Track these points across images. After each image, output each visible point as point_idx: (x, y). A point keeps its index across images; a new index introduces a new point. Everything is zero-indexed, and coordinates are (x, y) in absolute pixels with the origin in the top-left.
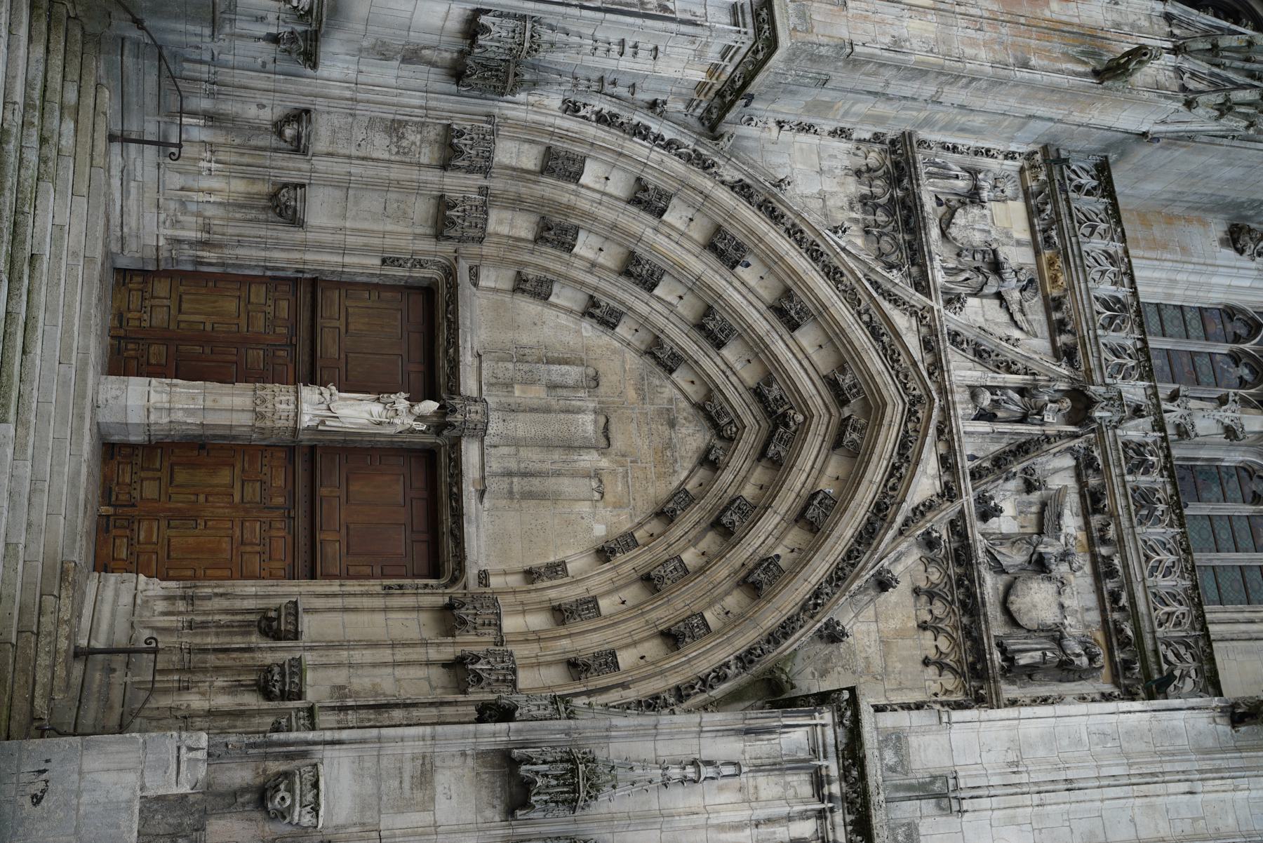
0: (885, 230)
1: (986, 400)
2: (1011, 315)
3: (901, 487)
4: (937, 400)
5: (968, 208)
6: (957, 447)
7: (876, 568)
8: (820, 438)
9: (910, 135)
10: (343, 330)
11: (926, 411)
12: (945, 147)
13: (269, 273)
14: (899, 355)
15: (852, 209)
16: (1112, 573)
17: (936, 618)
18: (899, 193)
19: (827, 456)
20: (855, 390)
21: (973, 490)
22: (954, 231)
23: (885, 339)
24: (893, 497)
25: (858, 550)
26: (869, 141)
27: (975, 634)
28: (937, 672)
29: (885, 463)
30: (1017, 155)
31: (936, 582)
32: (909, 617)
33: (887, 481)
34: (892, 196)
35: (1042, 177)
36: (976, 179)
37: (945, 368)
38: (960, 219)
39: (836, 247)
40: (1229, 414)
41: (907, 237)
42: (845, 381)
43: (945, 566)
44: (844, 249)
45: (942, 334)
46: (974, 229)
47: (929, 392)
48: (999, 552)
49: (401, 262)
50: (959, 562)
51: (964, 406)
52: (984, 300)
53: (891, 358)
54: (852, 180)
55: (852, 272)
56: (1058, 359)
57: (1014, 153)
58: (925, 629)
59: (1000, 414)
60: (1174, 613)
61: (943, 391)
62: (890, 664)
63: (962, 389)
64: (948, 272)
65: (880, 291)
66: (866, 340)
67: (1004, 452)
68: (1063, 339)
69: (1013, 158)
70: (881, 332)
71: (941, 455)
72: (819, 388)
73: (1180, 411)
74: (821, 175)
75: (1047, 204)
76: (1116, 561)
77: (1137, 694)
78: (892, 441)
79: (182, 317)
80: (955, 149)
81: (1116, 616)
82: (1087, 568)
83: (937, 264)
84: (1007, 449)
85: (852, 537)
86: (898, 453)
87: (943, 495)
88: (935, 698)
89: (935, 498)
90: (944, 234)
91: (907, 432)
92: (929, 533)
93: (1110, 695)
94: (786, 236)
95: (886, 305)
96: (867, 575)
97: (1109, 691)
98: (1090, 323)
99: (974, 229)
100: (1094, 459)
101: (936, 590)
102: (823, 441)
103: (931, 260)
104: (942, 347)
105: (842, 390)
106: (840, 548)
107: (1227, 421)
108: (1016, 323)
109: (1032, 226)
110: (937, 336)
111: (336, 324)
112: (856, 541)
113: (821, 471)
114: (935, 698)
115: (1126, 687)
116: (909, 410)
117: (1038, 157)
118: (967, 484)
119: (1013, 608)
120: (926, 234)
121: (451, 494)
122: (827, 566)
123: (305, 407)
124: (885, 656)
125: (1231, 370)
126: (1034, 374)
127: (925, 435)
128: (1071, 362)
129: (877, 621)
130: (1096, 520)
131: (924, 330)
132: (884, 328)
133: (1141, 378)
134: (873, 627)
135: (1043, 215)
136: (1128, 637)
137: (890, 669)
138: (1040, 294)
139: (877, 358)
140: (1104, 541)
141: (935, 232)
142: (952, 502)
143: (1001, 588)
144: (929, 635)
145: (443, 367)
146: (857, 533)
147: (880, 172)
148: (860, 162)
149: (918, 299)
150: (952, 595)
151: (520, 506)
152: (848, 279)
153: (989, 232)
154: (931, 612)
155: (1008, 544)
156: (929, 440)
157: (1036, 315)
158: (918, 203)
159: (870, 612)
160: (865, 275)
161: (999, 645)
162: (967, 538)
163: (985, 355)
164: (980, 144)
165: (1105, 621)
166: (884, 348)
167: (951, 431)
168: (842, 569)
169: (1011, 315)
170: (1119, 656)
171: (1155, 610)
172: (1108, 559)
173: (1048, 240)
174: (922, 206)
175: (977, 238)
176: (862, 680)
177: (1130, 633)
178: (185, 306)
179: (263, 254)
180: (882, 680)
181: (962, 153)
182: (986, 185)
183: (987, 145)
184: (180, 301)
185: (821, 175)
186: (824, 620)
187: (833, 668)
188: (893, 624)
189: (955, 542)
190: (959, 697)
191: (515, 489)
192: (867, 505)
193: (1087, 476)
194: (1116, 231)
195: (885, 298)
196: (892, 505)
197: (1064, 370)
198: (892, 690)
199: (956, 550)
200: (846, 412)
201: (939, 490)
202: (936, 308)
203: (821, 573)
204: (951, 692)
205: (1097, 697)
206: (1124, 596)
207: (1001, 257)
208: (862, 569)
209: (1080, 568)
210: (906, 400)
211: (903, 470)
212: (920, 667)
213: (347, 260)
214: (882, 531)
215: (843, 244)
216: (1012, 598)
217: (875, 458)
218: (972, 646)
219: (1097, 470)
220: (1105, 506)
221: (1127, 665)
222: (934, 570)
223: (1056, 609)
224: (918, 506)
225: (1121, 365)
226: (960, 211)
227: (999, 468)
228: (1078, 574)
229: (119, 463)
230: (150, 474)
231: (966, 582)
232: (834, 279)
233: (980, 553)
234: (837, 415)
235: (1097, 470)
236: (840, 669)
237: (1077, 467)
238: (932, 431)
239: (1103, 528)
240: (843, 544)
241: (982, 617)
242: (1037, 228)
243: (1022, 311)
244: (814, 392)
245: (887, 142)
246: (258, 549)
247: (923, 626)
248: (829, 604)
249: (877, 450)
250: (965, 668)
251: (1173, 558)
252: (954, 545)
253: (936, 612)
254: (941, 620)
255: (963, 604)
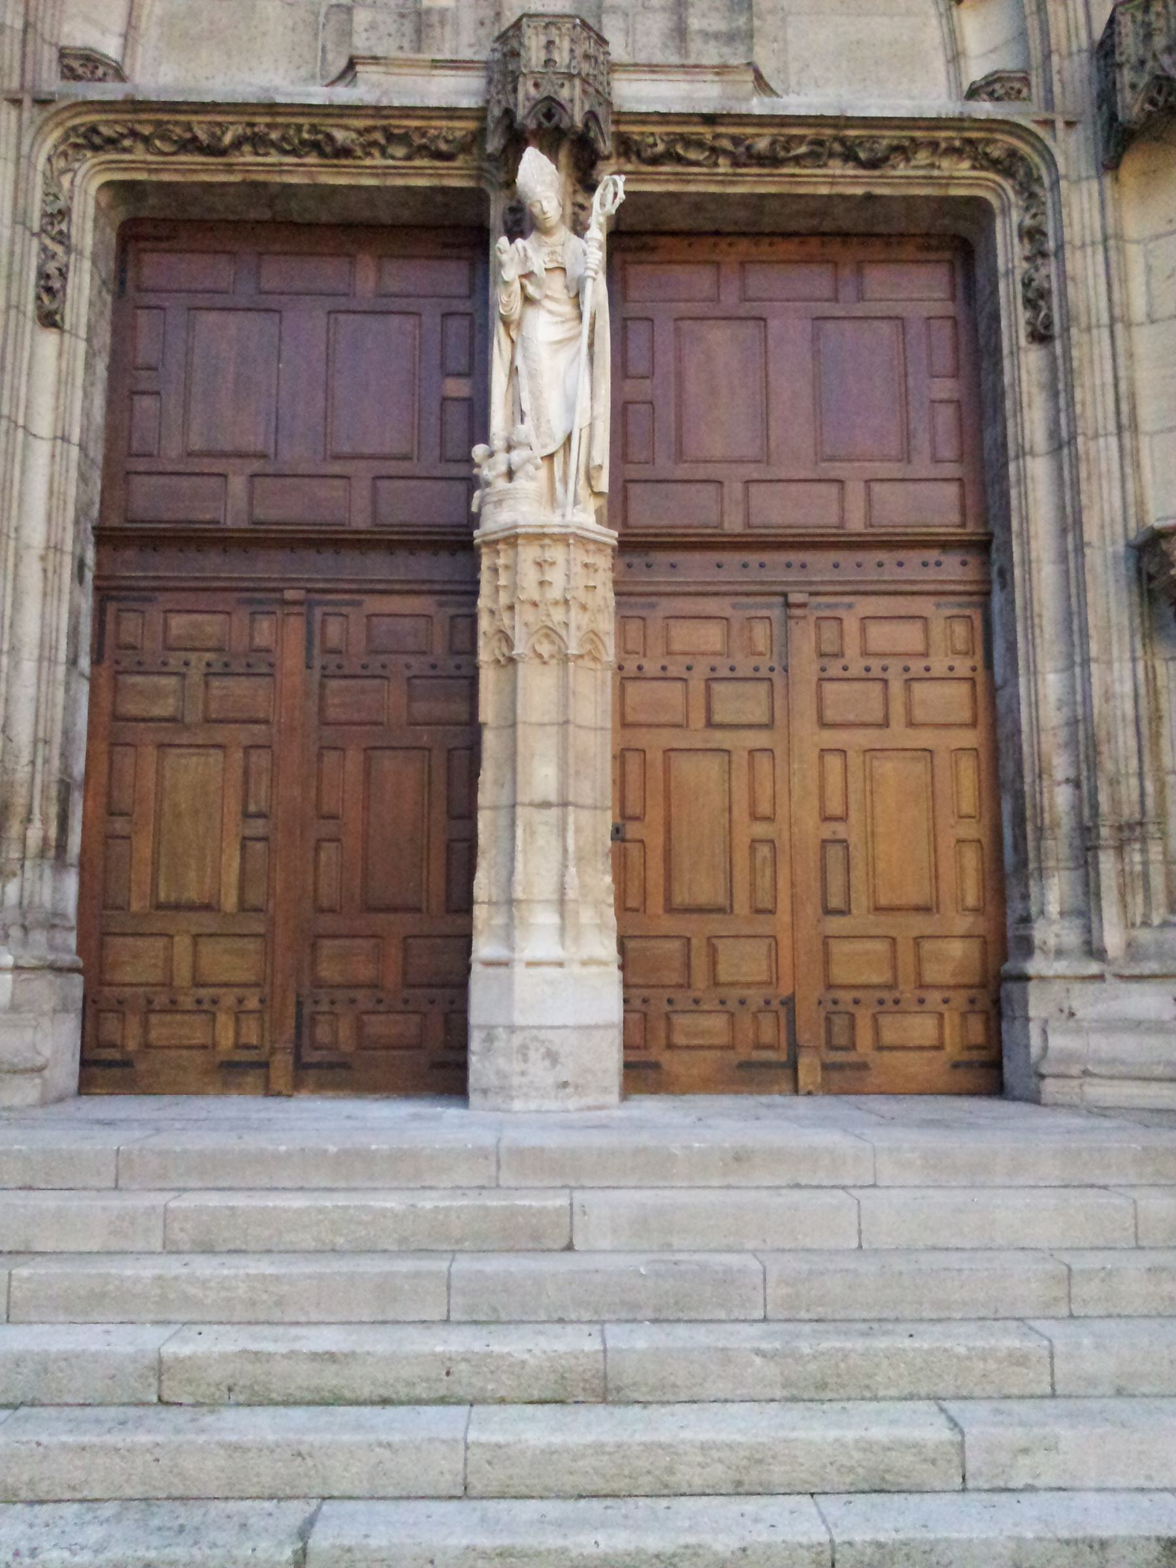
10: (256, 466)
13: (85, 663)
49: (51, 267)
79: (230, 901)
111: (237, 484)
121: (770, 160)
123: (552, 520)
145: (386, 172)
151: (772, 12)
178: (192, 894)
179: (28, 666)
184: (177, 907)
191: (717, 24)
213: (43, 424)
229: (670, 1046)
230: (699, 962)
246: (896, 687)
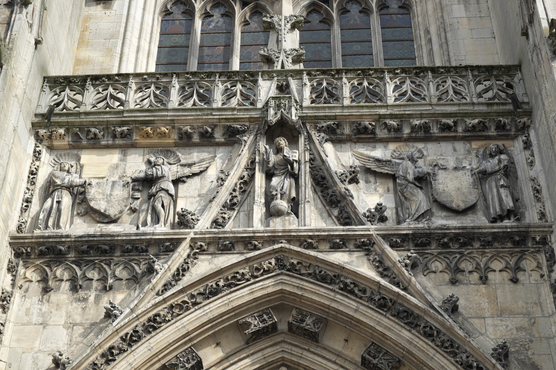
0: (109, 272)
1: (283, 204)
2: (194, 175)
3: (363, 284)
4: (280, 245)
5: (89, 197)
6: (326, 233)
7: (442, 313)
8: (305, 353)
9: (13, 238)
11: (290, 256)
12: (24, 210)
14: (238, 273)
15: (85, 300)
16: (426, 128)
17: (476, 268)
18: (72, 256)
19: (325, 349)
20: (265, 317)
21: (363, 224)
22: (112, 212)
23: (221, 283)
24: (372, 293)
25: (425, 327)
26: (14, 276)
27: (490, 239)
28: (522, 273)
29: (338, 296)
30: (38, 149)
31: (444, 265)
32: (478, 291)
33: (356, 296)
34: (73, 262)
35: (62, 131)
36: (62, 187)
37: (252, 235)
38: (100, 205)
39: (131, 317)
40: (283, 23)
41: (118, 253)
42: (255, 324)
43: (430, 257)
44: (132, 311)
45: (218, 233)
46: (111, 195)
47: (275, 251)
48: (417, 211)
50: (427, 244)
51: (287, 223)
52: (179, 195)
53: (239, 280)
54: (53, 296)
55: (156, 305)
56: (239, 142)
57: (35, 151)
58: (486, 278)
59: (294, 195)
60: (453, 88)
61: (273, 239)
62: (520, 311)
63: (271, 223)
64: (156, 219)
65: (173, 283)
66: (221, 300)
67: (323, 196)
68: (219, 137)
69: (39, 153)
70: (214, 286)
71: (331, 248)
72: (257, 349)
73: (282, 57)
74: (47, 325)
75: (90, 131)
76: (417, 122)
77: (524, 123)
78: (317, 288)
80: (28, 201)
81: (460, 129)
82: (420, 145)
83: (148, 229)
84: (320, 194)
85: (410, 331)
86: (330, 284)
87: (368, 250)
88: (546, 277)
89: (371, 258)
90: (114, 221)
91: (310, 274)
92: (406, 266)
93: (525, 143)
94: (113, 364)
95: (187, 280)
96: (450, 322)
97: (522, 144)
98: (206, 112)
99: (111, 195)
100: (328, 127)
101: (452, 265)
102: (308, 350)
103: (145, 234)
104: (231, 235)
105: (263, 328)
106: (421, 343)
107: (289, 26)
108: (201, 172)
109: (107, 147)
110: (220, 238)
112: (414, 328)
113: (339, 355)
114: (546, 277)
115: (518, 130)
116: (288, 270)
117: (42, 132)
118: (357, 229)
119: (462, 206)
120: (118, 236)
122: (438, 355)
124: (512, 313)
125: (216, 21)
126: (253, 162)
127: (316, 258)
128: (243, 132)
129: (484, 318)
130: (381, 133)
131: (212, 249)
132: (212, 283)
133: (255, 82)
134: (489, 321)
135: (100, 135)
136: (480, 123)
137: (524, 311)
138: (174, 149)
139: (238, 292)
140: (398, 130)
141: (112, 228)
142: (374, 243)
143: (444, 214)
144: (491, 275)
146: (406, 327)
147: (47, 269)
148: (36, 287)
149: (183, 250)
150: (455, 253)
152: (162, 310)
153: (114, 183)
154: (470, 272)
155: (407, 204)
156: (320, 255)
157: (195, 155)
158: (86, 239)
159: (476, 322)
160: (158, 294)
161: (494, 220)
162: (407, 235)
163: (235, 200)
164: (26, 179)
165: (463, 139)
166: (229, 286)
167: (310, 237)
168: (443, 342)
169: (194, 175)
170: (492, 132)
171: (452, 100)
172: (413, 128)
173: (123, 135)
174: (89, 236)
175: (120, 193)
176: (537, 335)
177: (476, 121)
180: (535, 318)
181: (32, 195)
182: (68, 179)
183: (27, 173)
185: (47, 325)
186: (494, 361)
187: (530, 359)
188: (485, 305)
189: (408, 245)
190: (542, 258)
192: (379, 316)
193: (343, 134)
194: (117, 80)
195: (180, 280)
196: (380, 294)
197: (249, 139)
198: (542, 311)
199: (416, 245)
200: (283, 327)
201: (362, 254)
202: (192, 235)
203: (446, 361)
204: (538, 263)
205: (528, 153)
206: (444, 121)
207: (142, 175)
208: (443, 324)
209: (420, 151)
210: (278, 272)
211: (348, 281)
212: (519, 287)
214: (406, 304)
215: (127, 311)
216: (454, 206)
217: (334, 305)
218: (498, 242)
219: (338, 125)
220: (370, 124)
221: (500, 127)
222: (433, 265)
223: (460, 173)
224: (378, 272)
225: (242, 94)
226: (92, 204)
227: (339, 202)
228: (425, 153)
231: (446, 240)
232: (161, 323)
233: (421, 225)
234: (283, 335)
235: (338, 125)
236: (530, 353)
237: (333, 142)
238: (312, 253)
239: (389, 128)
240: (417, 340)
241: (476, 231)
242: (110, 142)
243: (190, 165)
244: (260, 354)
245: (17, 261)
247: (484, 280)
248: (477, 356)
249: (327, 303)
250: (517, 250)
251: (408, 82)
252: (411, 246)
253: (470, 268)
254: (478, 264)
255: (463, 245)
